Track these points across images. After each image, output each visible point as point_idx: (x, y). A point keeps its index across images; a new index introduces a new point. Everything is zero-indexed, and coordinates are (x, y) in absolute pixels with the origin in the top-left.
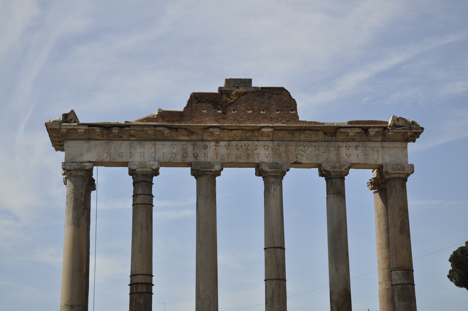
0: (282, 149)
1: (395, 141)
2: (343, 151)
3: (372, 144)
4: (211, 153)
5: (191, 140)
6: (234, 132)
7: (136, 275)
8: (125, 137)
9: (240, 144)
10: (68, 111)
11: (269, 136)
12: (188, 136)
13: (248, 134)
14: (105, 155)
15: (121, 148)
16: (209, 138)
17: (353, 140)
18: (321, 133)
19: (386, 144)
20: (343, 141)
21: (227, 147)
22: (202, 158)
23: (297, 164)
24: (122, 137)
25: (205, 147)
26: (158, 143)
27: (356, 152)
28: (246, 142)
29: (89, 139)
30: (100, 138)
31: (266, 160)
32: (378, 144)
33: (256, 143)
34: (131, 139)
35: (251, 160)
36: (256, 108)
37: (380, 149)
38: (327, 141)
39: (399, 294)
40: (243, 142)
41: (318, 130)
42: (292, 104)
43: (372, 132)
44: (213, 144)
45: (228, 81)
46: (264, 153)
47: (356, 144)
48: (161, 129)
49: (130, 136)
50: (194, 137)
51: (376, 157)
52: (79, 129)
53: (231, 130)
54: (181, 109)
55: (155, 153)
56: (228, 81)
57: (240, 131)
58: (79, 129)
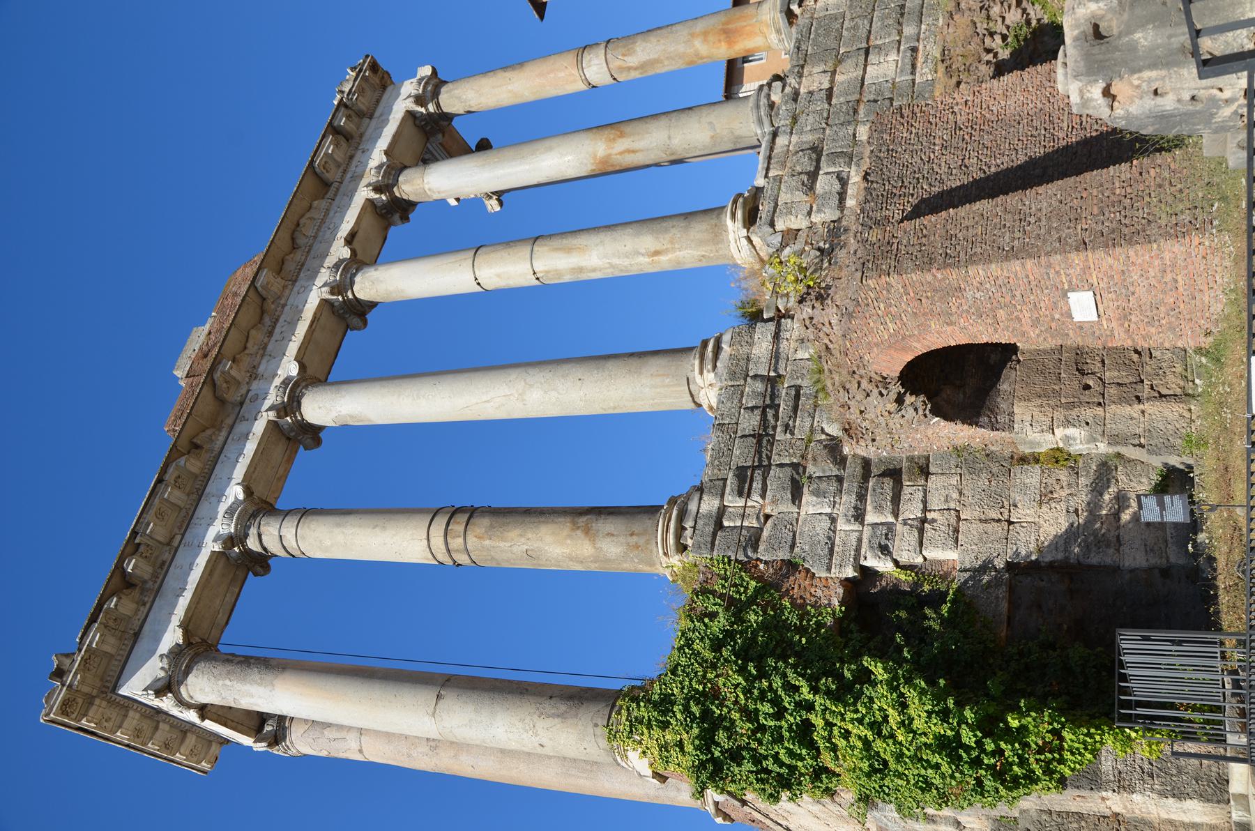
1: (378, 101)
6: (249, 345)
8: (167, 556)
9: (274, 338)
11: (285, 287)
12: (220, 430)
13: (267, 320)
16: (243, 391)
17: (351, 157)
18: (316, 203)
19: (377, 114)
24: (163, 563)
29: (137, 635)
30: (144, 610)
33: (287, 308)
34: (175, 543)
38: (335, 195)
39: (624, 55)
40: (277, 330)
41: (310, 207)
48: (171, 470)
49: (169, 544)
52: (91, 642)
53: (245, 348)
57: (253, 332)
58: (91, 642)
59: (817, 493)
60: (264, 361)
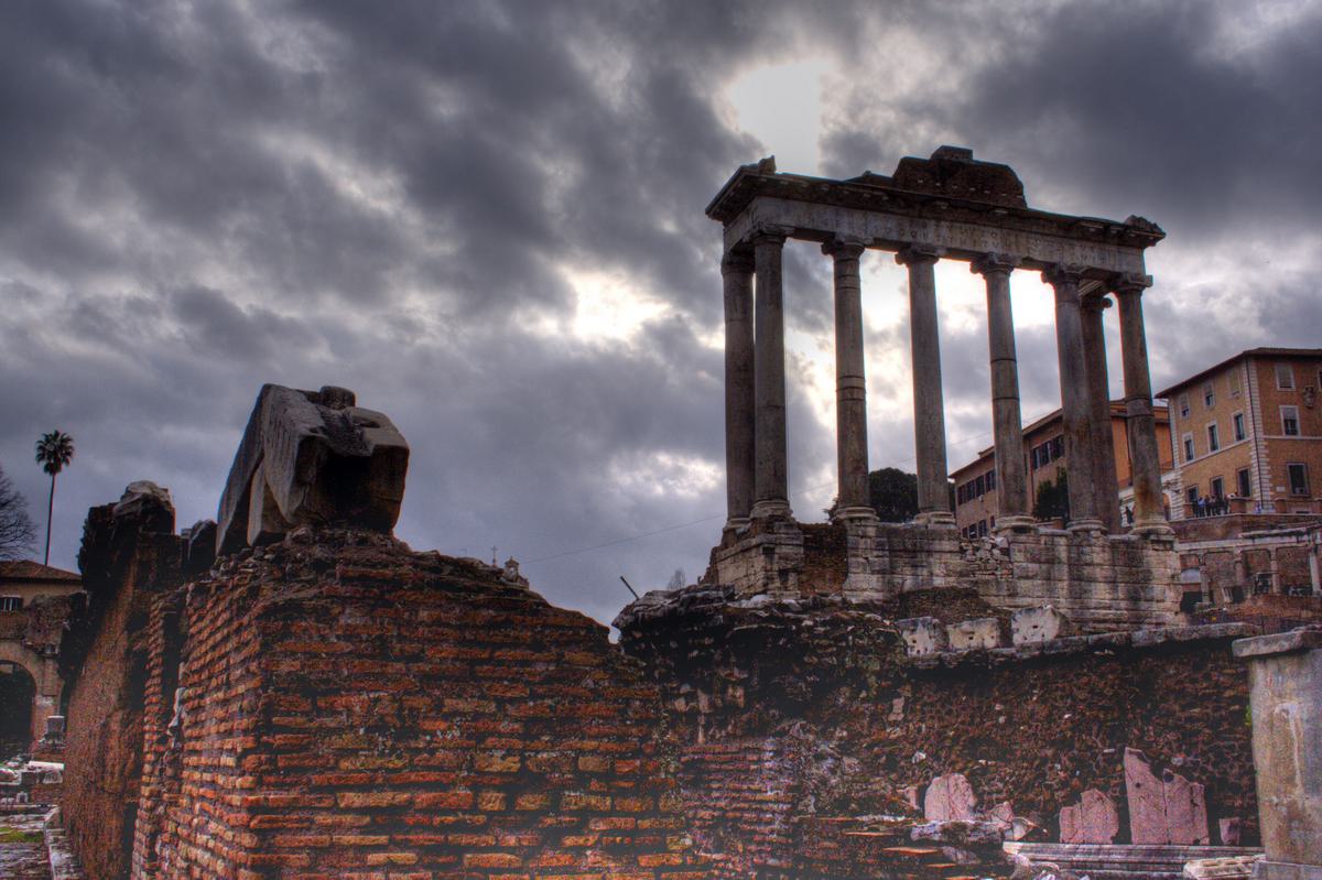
0: (1013, 239)
4: (930, 235)
5: (906, 215)
6: (959, 211)
7: (845, 377)
14: (807, 221)
15: (825, 218)
20: (1078, 239)
21: (950, 228)
22: (921, 239)
23: (1029, 263)
25: (925, 226)
26: (871, 216)
31: (995, 250)
32: (1113, 248)
33: (983, 228)
35: (977, 249)
36: (980, 186)
40: (968, 226)
42: (1016, 188)
44: (933, 222)
46: (991, 244)
48: (880, 193)
53: (956, 208)
55: (866, 225)
59: (878, 581)
60: (948, 223)
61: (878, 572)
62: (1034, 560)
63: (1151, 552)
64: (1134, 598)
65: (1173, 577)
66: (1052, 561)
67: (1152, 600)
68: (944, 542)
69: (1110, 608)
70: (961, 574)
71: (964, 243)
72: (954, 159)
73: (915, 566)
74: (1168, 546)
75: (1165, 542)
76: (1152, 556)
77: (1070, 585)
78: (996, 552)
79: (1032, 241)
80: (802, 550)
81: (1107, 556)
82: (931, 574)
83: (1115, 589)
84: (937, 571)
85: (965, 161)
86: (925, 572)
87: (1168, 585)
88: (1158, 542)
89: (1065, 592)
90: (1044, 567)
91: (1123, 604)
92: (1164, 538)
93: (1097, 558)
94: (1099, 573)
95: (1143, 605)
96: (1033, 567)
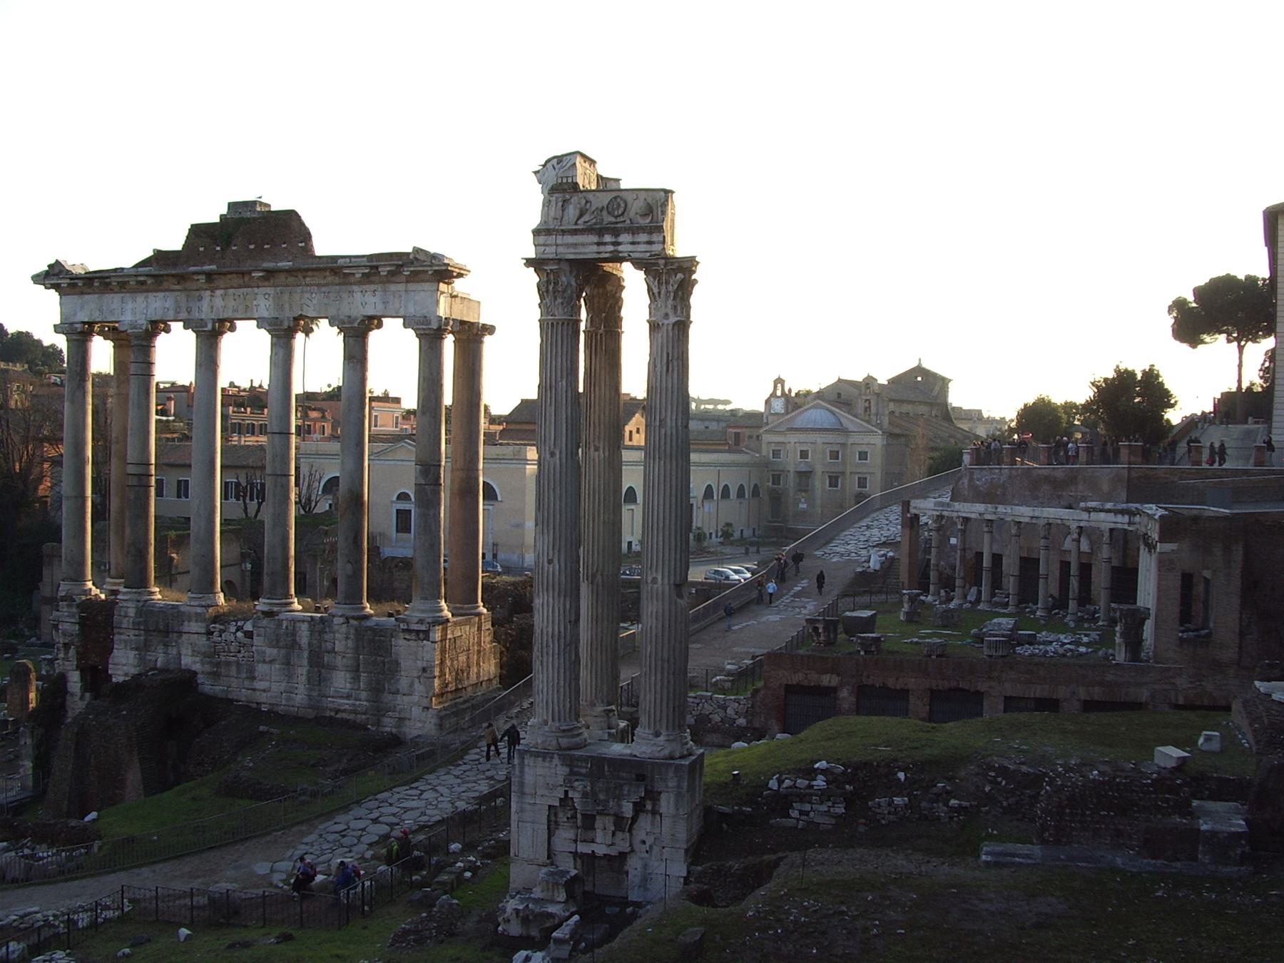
0: (286, 297)
2: (358, 296)
3: (393, 287)
10: (53, 262)
13: (246, 279)
19: (411, 286)
21: (224, 297)
22: (196, 315)
25: (200, 299)
27: (374, 300)
28: (245, 290)
29: (82, 293)
31: (265, 314)
32: (401, 287)
33: (256, 290)
35: (249, 315)
37: (403, 294)
38: (339, 284)
43: (384, 271)
44: (208, 293)
45: (232, 206)
46: (264, 302)
47: (373, 287)
50: (189, 285)
51: (397, 305)
54: (179, 248)
56: (232, 206)
61: (137, 649)
62: (275, 643)
63: (402, 642)
64: (377, 690)
65: (424, 670)
66: (293, 645)
67: (397, 692)
68: (193, 624)
69: (348, 697)
70: (205, 655)
71: (235, 311)
72: (237, 216)
73: (166, 645)
74: (421, 636)
75: (418, 632)
76: (402, 646)
77: (309, 672)
78: (240, 634)
79: (307, 295)
80: (77, 627)
81: (350, 643)
82: (179, 654)
83: (356, 679)
84: (184, 651)
85: (248, 215)
86: (174, 652)
87: (419, 677)
88: (409, 631)
89: (304, 678)
90: (283, 651)
91: (364, 695)
92: (415, 627)
93: (339, 647)
94: (339, 661)
95: (387, 697)
96: (271, 652)
